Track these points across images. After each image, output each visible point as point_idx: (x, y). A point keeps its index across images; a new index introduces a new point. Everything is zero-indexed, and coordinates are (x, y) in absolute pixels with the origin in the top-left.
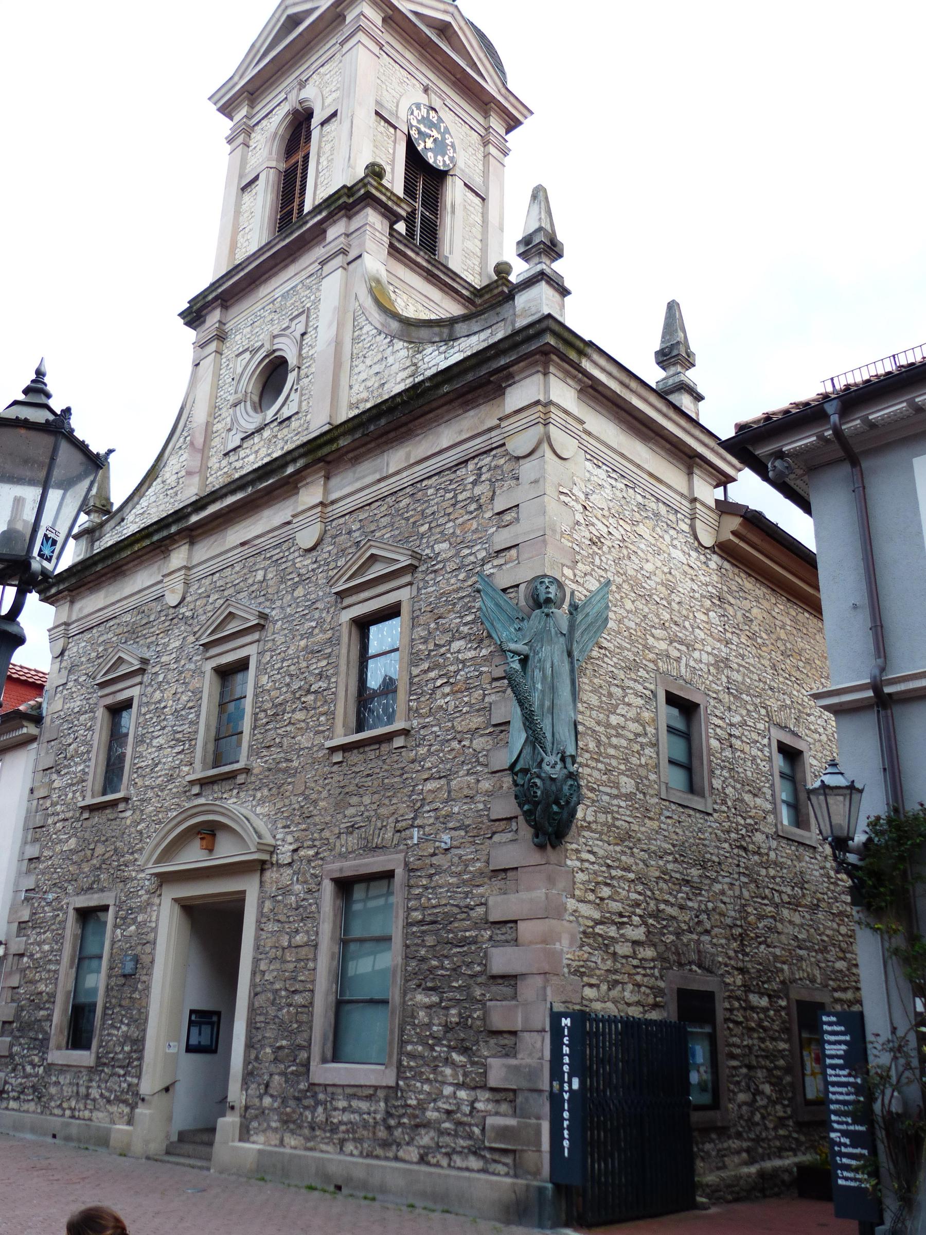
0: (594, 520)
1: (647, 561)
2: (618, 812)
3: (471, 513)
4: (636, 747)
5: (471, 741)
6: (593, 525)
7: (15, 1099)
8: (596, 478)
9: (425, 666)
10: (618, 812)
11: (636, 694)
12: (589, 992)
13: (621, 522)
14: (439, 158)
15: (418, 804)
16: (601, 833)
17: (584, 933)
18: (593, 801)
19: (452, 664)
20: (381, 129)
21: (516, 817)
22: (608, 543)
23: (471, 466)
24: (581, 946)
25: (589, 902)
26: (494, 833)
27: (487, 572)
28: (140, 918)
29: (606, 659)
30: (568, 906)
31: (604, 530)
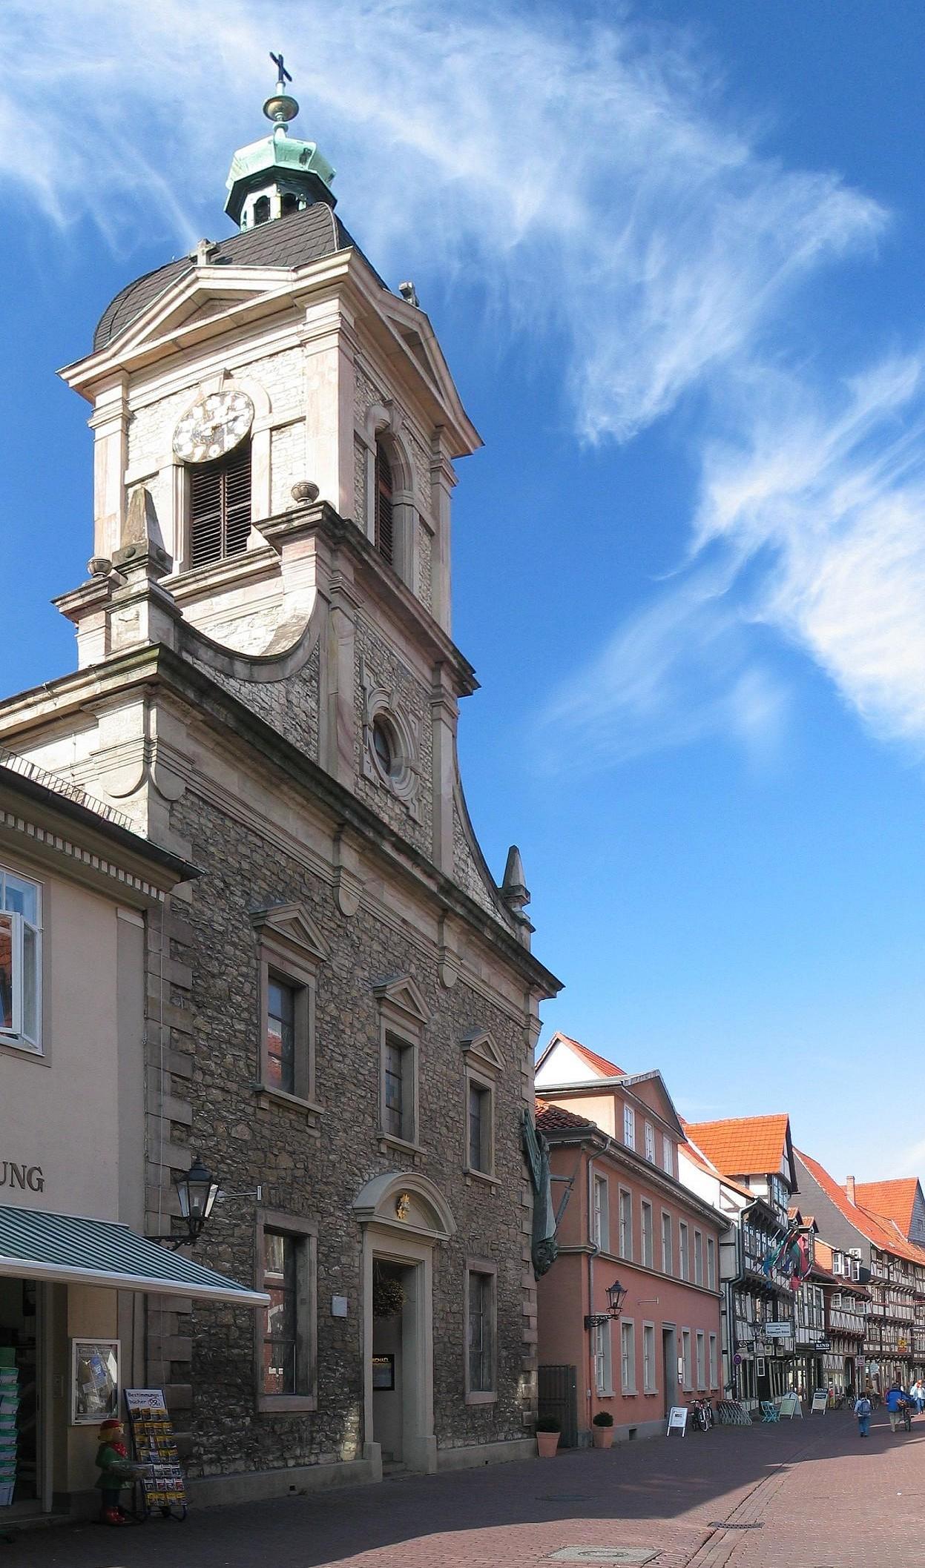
7: (211, 1462)
28: (344, 1260)
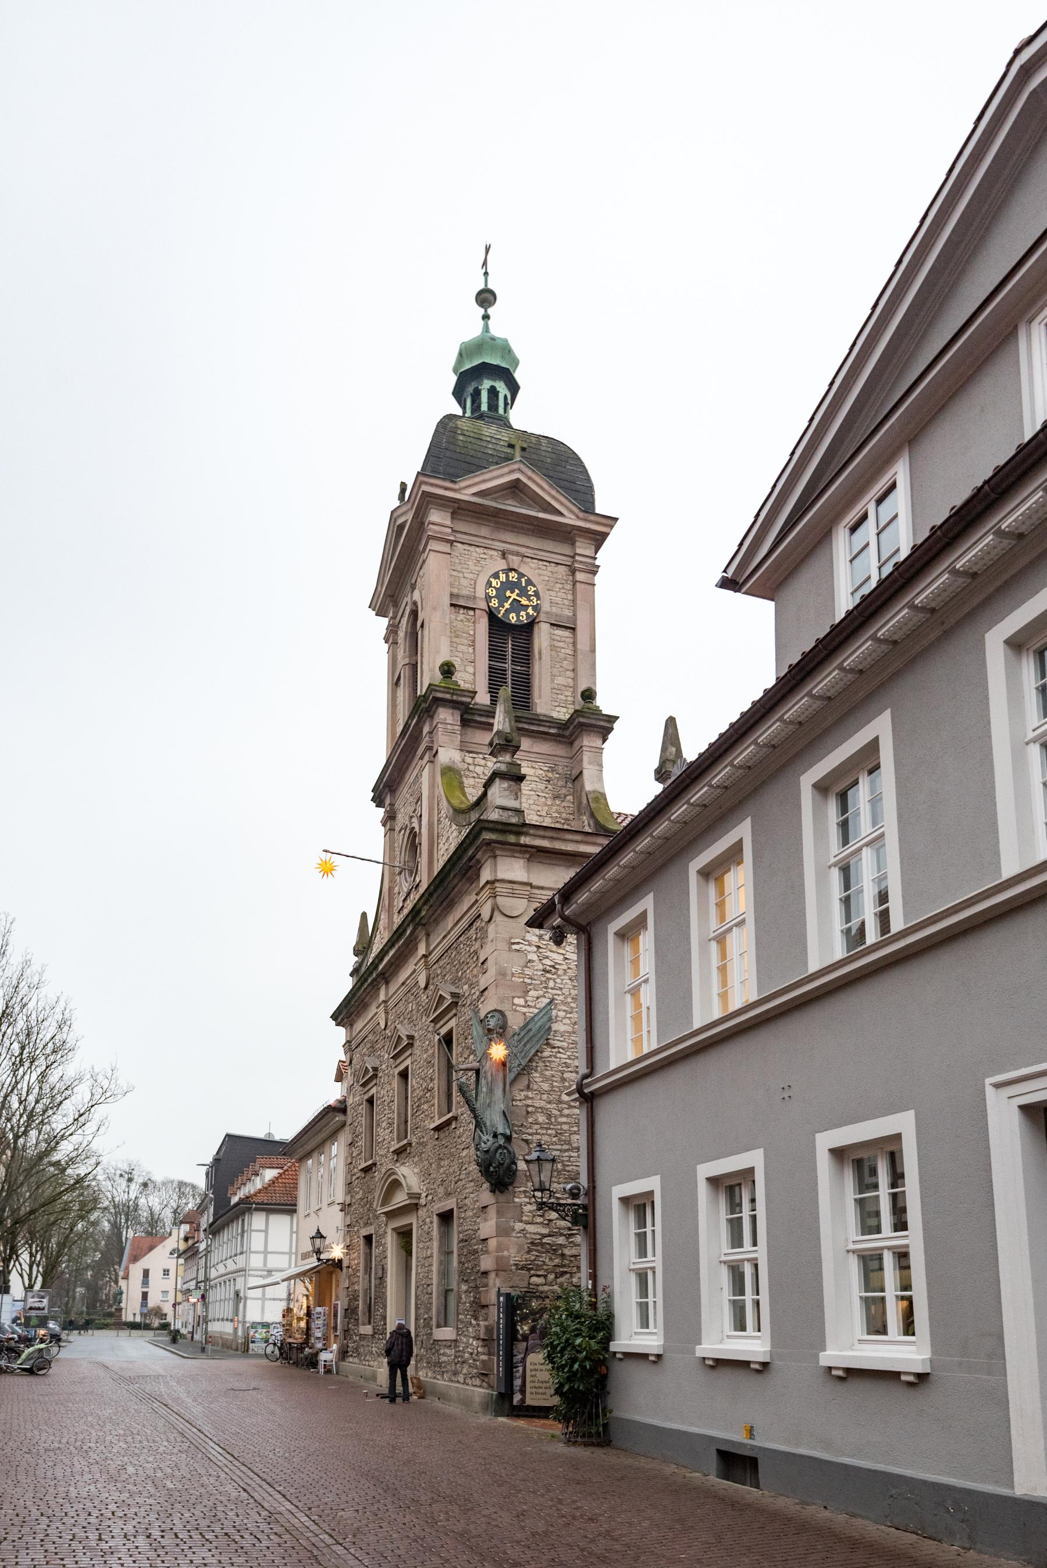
0: (549, 954)
2: (569, 1161)
6: (547, 957)
12: (534, 1280)
14: (523, 613)
17: (532, 1243)
20: (461, 617)
22: (565, 967)
24: (528, 1252)
25: (537, 1223)
30: (516, 1227)
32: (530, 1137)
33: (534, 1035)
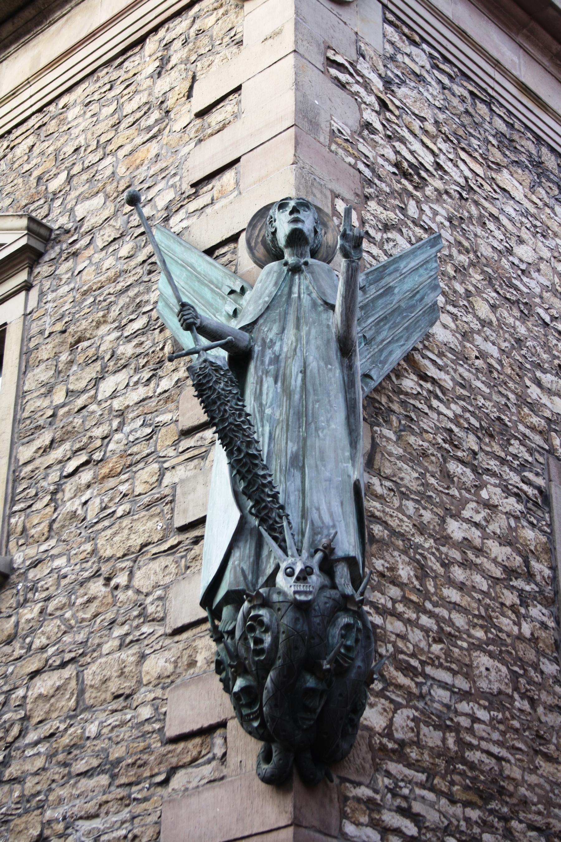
1: (521, 241)
2: (471, 730)
3: (149, 129)
4: (510, 598)
5: (131, 574)
6: (402, 140)
8: (407, 60)
9: (45, 438)
10: (471, 730)
11: (507, 490)
13: (463, 155)
15: (15, 731)
16: (431, 773)
18: (410, 696)
19: (98, 424)
21: (223, 725)
22: (438, 184)
23: (151, 45)
26: (173, 771)
27: (177, 229)
29: (435, 403)
31: (428, 160)
32: (378, 620)
33: (397, 310)
